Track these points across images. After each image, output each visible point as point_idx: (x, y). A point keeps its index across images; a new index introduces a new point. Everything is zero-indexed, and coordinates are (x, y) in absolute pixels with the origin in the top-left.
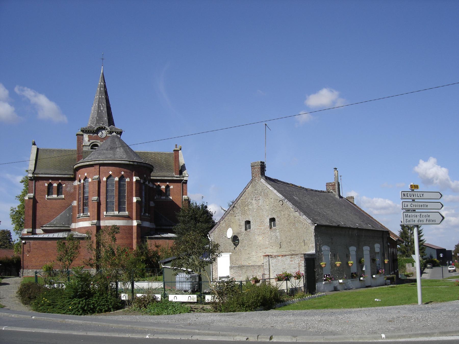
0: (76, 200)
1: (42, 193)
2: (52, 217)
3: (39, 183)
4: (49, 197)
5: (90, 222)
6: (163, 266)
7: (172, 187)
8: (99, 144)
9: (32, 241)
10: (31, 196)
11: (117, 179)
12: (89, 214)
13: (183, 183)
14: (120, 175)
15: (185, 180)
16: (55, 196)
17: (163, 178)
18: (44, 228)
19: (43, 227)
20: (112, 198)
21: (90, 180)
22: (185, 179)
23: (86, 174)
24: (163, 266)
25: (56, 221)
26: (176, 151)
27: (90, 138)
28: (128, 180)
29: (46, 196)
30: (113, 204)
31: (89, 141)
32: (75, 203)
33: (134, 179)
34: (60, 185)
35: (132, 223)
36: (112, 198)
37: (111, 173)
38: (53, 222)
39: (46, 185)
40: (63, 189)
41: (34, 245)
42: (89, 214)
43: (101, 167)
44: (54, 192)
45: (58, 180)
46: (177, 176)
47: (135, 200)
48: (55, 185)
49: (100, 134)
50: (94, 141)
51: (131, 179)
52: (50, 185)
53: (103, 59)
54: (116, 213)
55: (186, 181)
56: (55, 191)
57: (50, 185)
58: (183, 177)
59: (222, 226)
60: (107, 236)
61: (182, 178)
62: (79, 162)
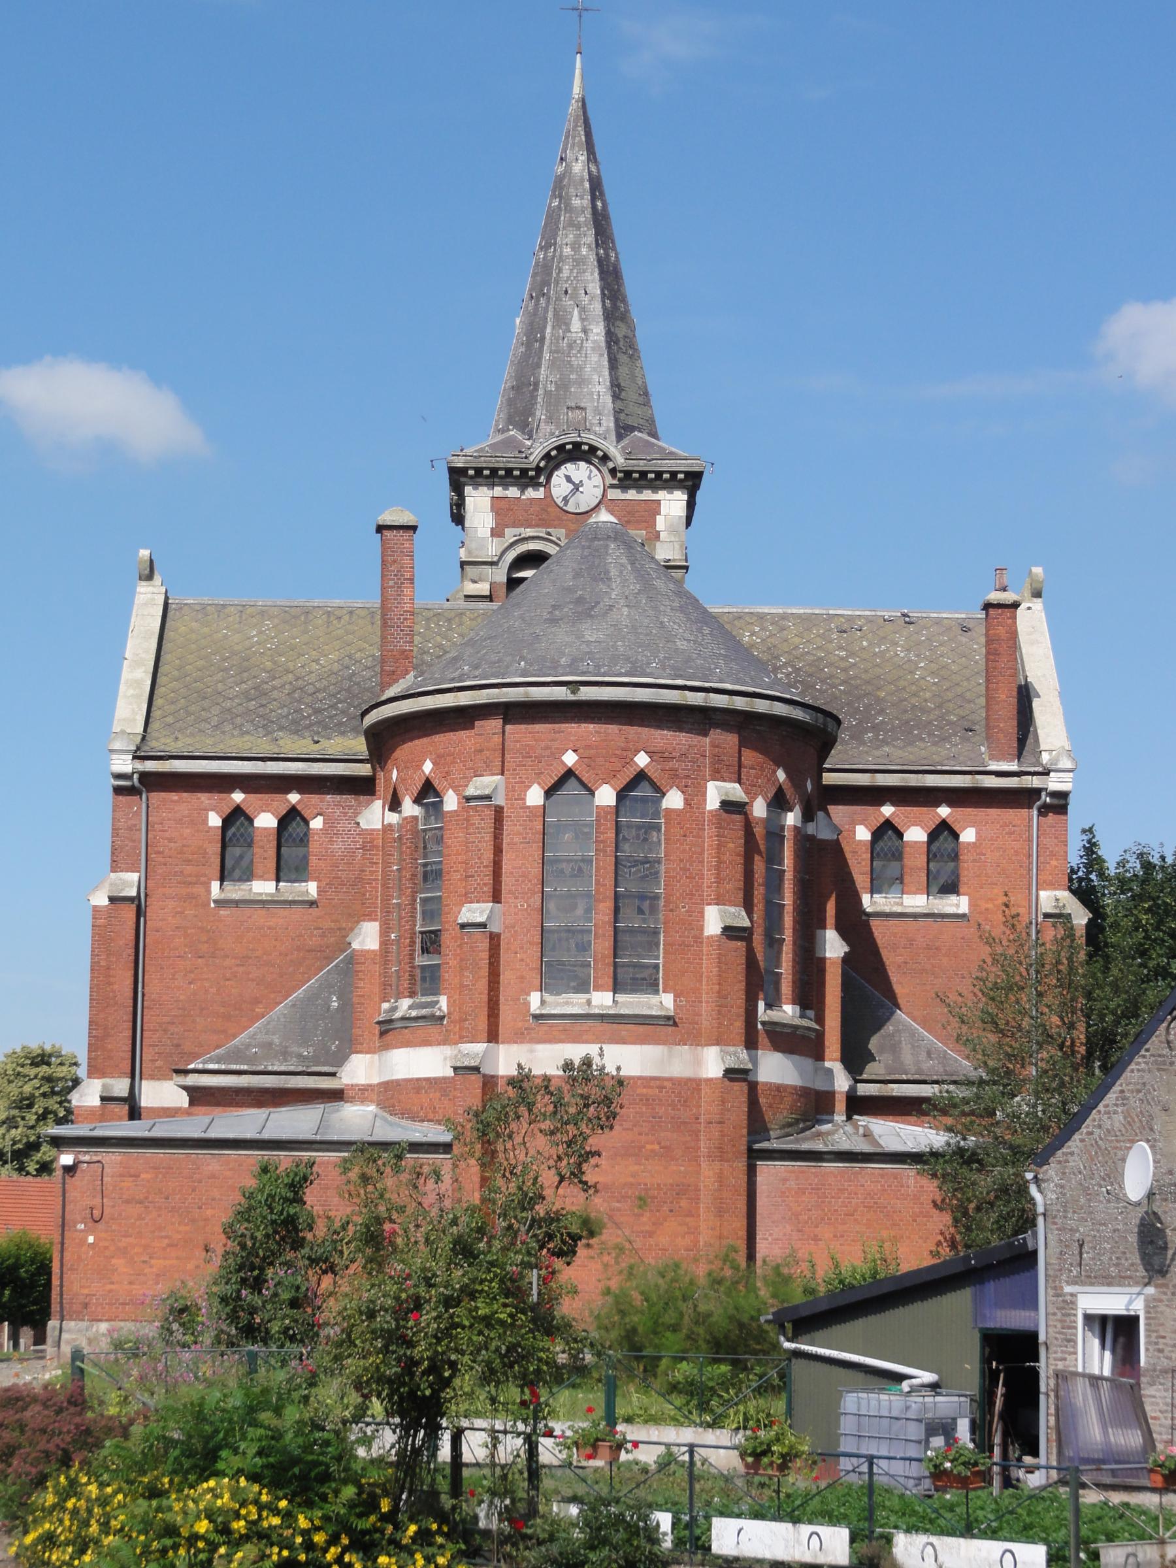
0: (370, 917)
1: (189, 869)
2: (245, 1011)
3: (174, 806)
4: (235, 891)
5: (448, 1050)
6: (787, 1345)
7: (968, 836)
8: (551, 549)
9: (112, 1158)
10: (126, 884)
11: (606, 796)
12: (443, 1001)
13: (1045, 810)
14: (630, 773)
15: (1055, 794)
16: (263, 887)
17: (913, 781)
18: (192, 1080)
19: (186, 1072)
20: (580, 911)
21: (451, 802)
22: (1054, 783)
23: (428, 767)
24: (787, 1345)
25: (265, 1038)
26: (1001, 612)
27: (503, 514)
28: (674, 800)
29: (215, 886)
30: (584, 948)
31: (496, 533)
32: (367, 937)
33: (715, 793)
34: (290, 818)
35: (698, 1062)
36: (580, 911)
37: (570, 759)
38: (248, 1046)
39: (215, 820)
40: (314, 847)
41: (128, 1183)
42: (443, 1001)
43: (508, 727)
44: (258, 868)
45: (288, 791)
46: (1005, 766)
47: (713, 921)
48: (266, 821)
49: (559, 485)
50: (530, 532)
51: (694, 796)
52: (236, 817)
53: (580, 11)
54: (602, 1000)
55: (1063, 795)
56: (265, 854)
57: (236, 817)
58: (1046, 773)
59: (1107, 1124)
60: (541, 1142)
61: (1036, 782)
62: (391, 693)
